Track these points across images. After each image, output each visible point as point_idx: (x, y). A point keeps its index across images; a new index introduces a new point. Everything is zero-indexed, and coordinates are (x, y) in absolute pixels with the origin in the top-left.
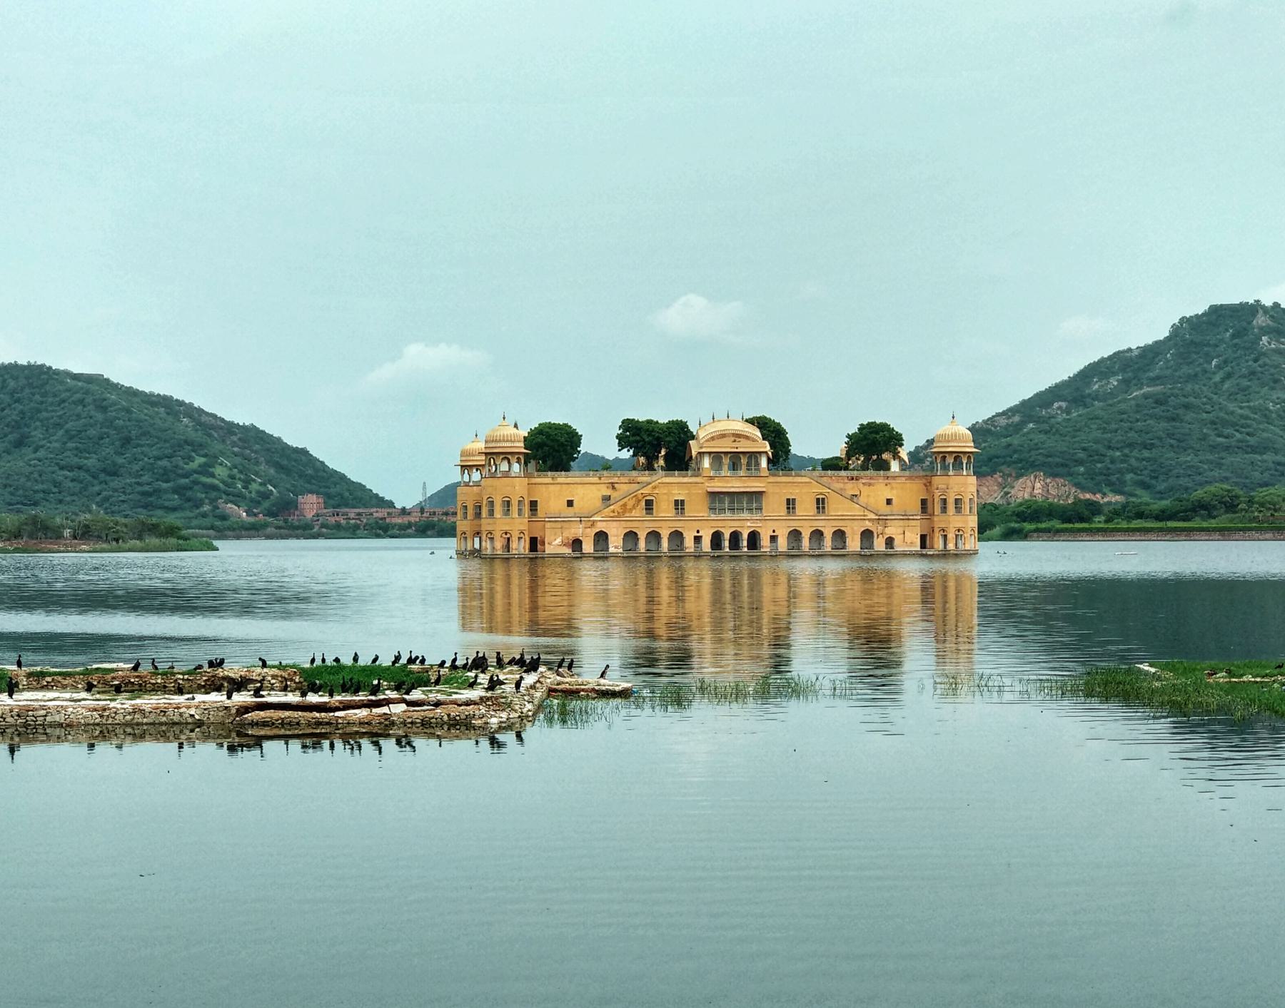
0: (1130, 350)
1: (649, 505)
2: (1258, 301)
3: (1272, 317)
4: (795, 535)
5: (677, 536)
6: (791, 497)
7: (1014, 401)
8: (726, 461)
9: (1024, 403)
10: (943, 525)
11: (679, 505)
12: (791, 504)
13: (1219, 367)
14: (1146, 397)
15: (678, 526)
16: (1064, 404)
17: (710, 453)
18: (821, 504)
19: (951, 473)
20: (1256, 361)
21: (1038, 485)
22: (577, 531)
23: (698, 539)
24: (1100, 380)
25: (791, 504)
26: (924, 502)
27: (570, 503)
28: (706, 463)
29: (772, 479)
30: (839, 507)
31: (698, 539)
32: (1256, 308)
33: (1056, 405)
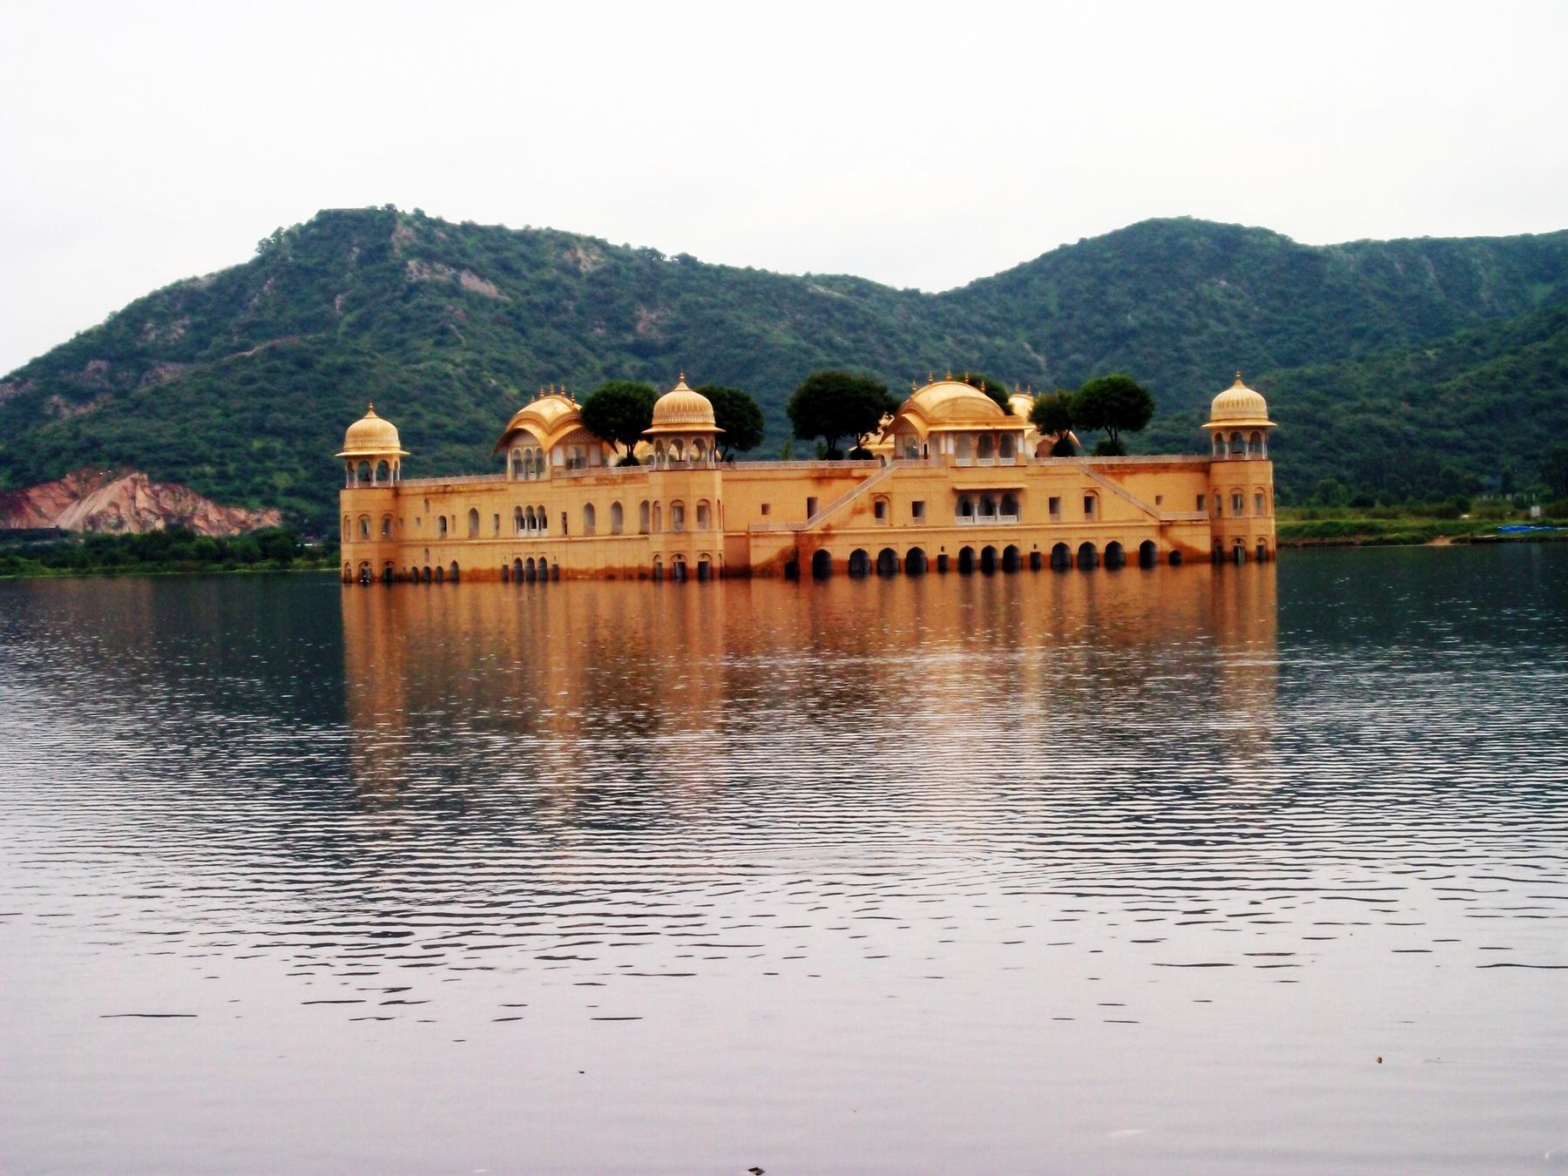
0: (195, 279)
2: (390, 207)
3: (418, 231)
7: (22, 361)
8: (974, 442)
9: (36, 363)
10: (1240, 533)
11: (917, 508)
12: (1053, 504)
13: (346, 309)
14: (273, 352)
16: (103, 365)
17: (954, 433)
18: (1088, 504)
19: (1247, 457)
20: (405, 299)
21: (140, 495)
24: (157, 327)
25: (1053, 504)
26: (1200, 499)
27: (765, 509)
28: (948, 447)
32: (390, 214)
33: (92, 365)
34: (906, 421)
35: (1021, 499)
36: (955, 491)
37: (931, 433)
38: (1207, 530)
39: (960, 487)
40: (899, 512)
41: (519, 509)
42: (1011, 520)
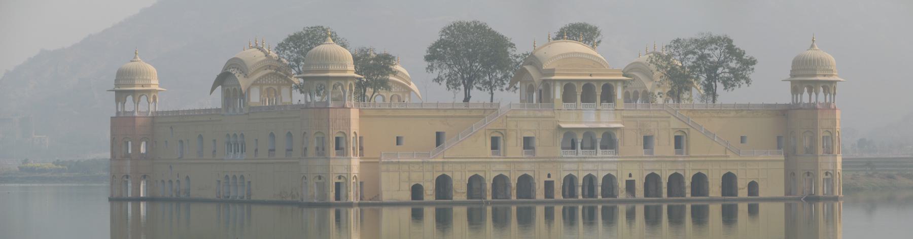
1: (495, 144)
4: (652, 180)
5: (525, 182)
6: (648, 134)
8: (579, 91)
11: (528, 143)
12: (647, 142)
15: (527, 169)
17: (561, 81)
18: (678, 142)
22: (416, 178)
23: (549, 185)
25: (647, 142)
27: (399, 141)
28: (558, 93)
29: (625, 114)
30: (697, 146)
31: (549, 185)
34: (525, 69)
35: (618, 136)
36: (559, 128)
37: (544, 81)
38: (782, 165)
39: (563, 126)
40: (513, 148)
41: (228, 135)
42: (608, 155)
